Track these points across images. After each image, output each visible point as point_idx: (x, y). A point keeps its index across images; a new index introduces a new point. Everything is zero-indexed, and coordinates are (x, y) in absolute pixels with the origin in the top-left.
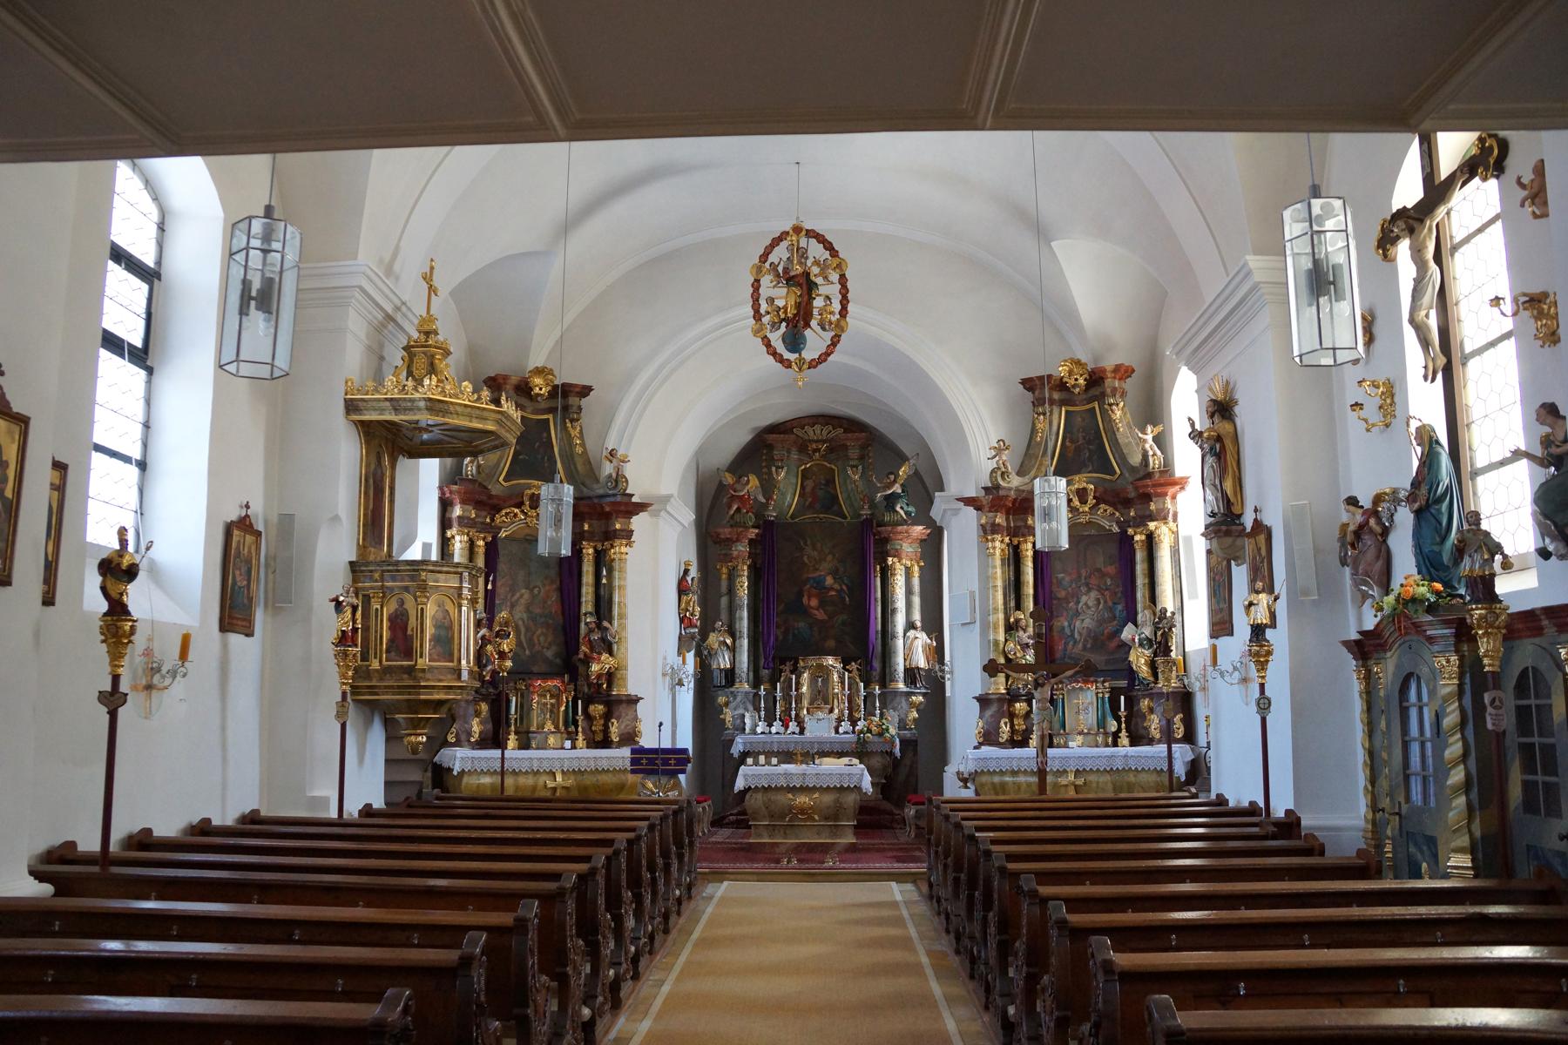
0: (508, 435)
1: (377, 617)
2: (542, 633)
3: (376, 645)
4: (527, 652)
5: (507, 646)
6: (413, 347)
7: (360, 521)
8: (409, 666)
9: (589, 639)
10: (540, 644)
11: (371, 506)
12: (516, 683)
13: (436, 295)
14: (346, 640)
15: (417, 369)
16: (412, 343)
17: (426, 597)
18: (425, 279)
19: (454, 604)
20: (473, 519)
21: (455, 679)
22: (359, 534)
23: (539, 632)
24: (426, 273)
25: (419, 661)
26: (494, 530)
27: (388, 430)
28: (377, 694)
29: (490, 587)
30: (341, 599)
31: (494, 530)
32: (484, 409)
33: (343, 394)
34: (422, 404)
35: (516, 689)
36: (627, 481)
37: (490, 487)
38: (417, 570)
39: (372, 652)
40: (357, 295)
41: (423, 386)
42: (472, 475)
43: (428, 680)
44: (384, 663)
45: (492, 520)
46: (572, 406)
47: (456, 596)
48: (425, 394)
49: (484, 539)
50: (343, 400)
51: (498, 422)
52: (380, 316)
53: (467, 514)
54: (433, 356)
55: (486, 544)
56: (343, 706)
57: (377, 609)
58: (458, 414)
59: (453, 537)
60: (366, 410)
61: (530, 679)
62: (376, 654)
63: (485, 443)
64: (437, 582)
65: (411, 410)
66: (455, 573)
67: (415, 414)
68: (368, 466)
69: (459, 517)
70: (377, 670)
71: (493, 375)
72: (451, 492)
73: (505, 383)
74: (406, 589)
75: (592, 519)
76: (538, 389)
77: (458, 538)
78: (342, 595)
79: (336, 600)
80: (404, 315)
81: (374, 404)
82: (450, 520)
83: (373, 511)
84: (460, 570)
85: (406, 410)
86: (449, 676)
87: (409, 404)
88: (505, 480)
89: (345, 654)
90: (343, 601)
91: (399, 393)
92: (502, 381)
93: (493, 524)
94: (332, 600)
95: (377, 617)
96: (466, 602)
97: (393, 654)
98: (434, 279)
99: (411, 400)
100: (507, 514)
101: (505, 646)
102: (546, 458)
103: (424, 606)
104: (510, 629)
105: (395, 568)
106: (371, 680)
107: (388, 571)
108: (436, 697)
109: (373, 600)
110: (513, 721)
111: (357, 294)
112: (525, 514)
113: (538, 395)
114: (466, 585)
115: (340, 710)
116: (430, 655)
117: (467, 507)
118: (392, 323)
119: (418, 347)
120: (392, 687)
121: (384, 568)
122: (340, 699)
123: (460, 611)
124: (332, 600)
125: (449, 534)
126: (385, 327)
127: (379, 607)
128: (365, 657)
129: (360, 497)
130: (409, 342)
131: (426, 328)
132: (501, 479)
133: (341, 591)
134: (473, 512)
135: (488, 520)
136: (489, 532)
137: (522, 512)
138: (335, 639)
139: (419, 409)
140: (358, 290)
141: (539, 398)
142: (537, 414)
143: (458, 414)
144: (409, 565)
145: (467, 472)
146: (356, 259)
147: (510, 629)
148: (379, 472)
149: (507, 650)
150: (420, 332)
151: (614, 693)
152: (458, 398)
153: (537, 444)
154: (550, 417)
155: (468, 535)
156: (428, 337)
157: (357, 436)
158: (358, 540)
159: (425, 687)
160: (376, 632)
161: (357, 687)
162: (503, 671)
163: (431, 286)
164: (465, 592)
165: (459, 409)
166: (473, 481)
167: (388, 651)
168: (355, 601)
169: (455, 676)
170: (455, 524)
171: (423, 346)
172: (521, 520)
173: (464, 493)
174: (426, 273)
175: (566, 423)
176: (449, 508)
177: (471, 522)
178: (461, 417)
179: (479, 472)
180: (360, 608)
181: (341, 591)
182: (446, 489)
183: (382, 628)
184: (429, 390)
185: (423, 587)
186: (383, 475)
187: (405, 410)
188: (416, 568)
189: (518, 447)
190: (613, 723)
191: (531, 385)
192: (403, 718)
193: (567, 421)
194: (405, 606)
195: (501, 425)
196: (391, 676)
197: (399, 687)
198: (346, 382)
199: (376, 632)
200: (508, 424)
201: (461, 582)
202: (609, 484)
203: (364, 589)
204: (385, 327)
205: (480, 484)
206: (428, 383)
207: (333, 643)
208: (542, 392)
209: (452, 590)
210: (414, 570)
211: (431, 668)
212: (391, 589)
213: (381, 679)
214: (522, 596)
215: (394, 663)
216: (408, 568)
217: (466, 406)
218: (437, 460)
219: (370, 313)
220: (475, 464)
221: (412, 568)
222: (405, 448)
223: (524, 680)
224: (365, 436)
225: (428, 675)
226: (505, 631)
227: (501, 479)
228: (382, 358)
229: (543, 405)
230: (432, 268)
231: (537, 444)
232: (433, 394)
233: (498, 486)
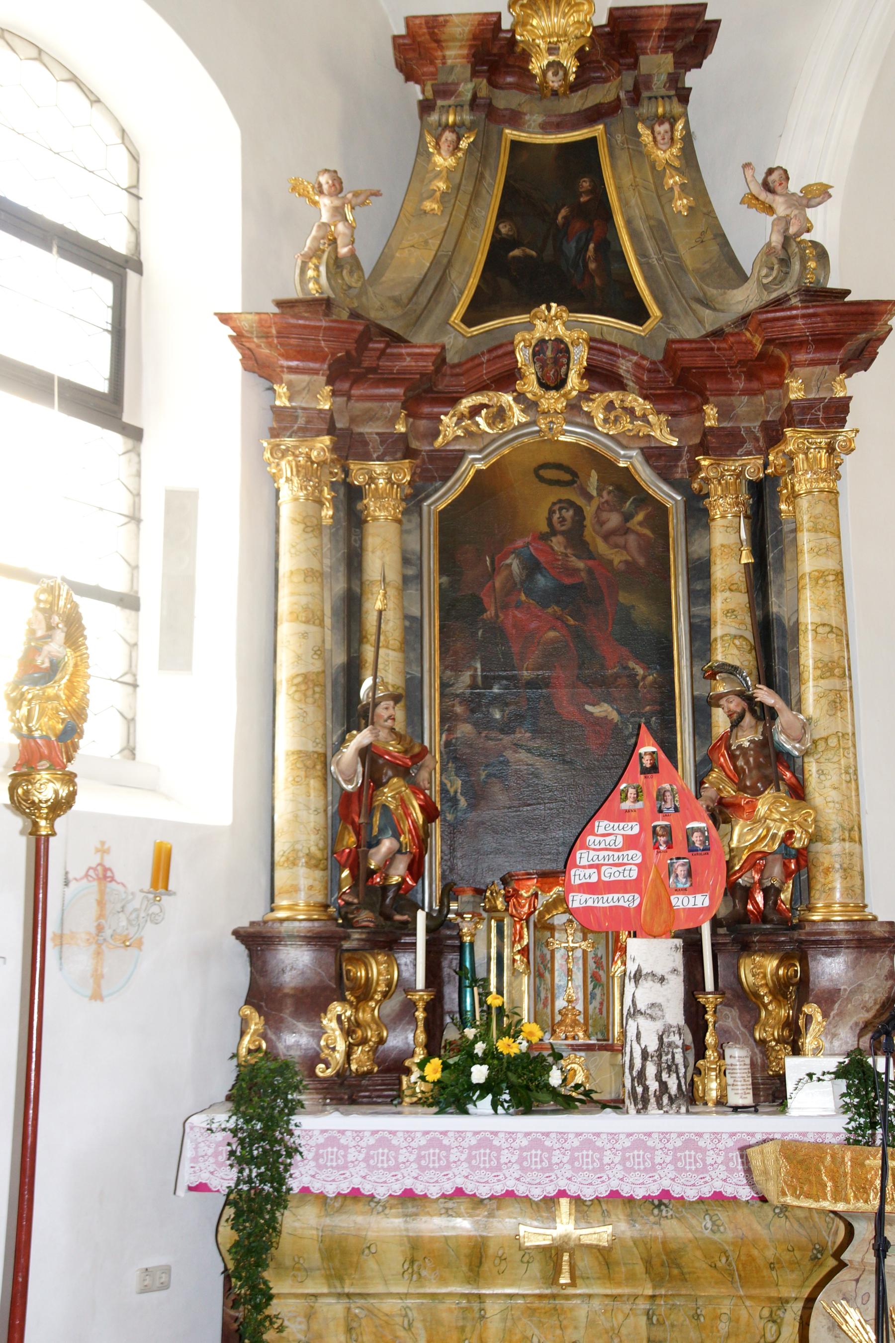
9: (728, 748)
36: (822, 255)
46: (648, 78)
75: (729, 393)
88: (469, 320)
100: (475, 411)
112: (530, 406)
137: (520, 398)
141: (554, 82)
142: (559, 126)
151: (816, 917)
153: (563, 212)
154: (598, 130)
172: (522, 425)
175: (639, 135)
189: (504, 229)
190: (809, 1019)
193: (641, 128)
202: (764, 271)
229: (577, 102)
231: (563, 212)
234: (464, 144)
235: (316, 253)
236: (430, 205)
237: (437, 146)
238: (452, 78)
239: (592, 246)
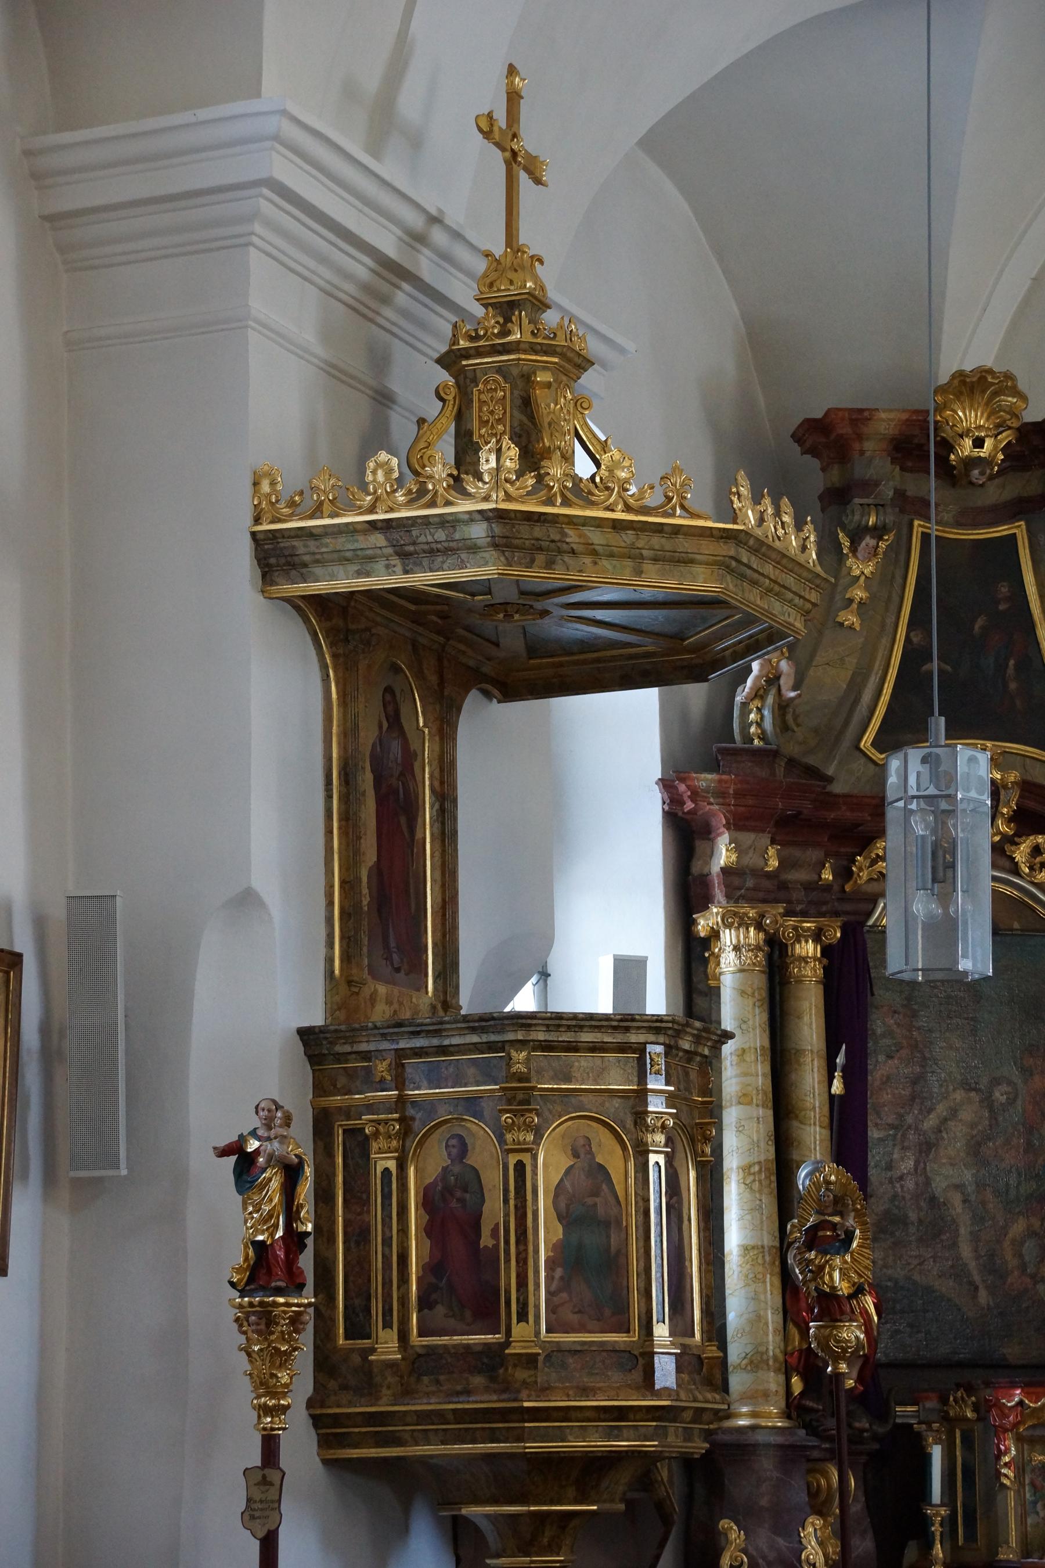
0: (777, 607)
1: (387, 1196)
2: (1031, 1233)
3: (387, 1283)
4: (983, 1296)
5: (844, 1274)
6: (466, 354)
7: (330, 904)
8: (487, 1345)
10: (1023, 1267)
11: (370, 855)
12: (944, 1400)
13: (538, 181)
14: (269, 1273)
15: (484, 423)
16: (463, 343)
17: (528, 1127)
18: (487, 135)
19: (624, 1147)
20: (768, 875)
21: (637, 1388)
22: (330, 945)
23: (1018, 1227)
24: (490, 116)
25: (519, 1330)
26: (848, 907)
27: (417, 619)
28: (394, 1440)
29: (837, 1087)
30: (253, 1145)
31: (848, 907)
32: (677, 530)
33: (249, 520)
34: (478, 531)
35: (946, 1418)
37: (830, 771)
38: (500, 1046)
39: (377, 1308)
40: (265, 207)
41: (479, 476)
42: (763, 737)
43: (544, 1391)
44: (416, 1340)
45: (845, 873)
47: (629, 1123)
48: (486, 499)
49: (817, 936)
50: (248, 540)
51: (729, 567)
52: (361, 268)
53: (752, 860)
54: (527, 378)
55: (827, 951)
56: (265, 1482)
57: (387, 1170)
58: (594, 553)
59: (715, 934)
60: (317, 561)
61: (988, 1384)
62: (387, 1312)
63: (721, 637)
64: (568, 1079)
65: (448, 551)
66: (623, 1048)
67: (462, 566)
68: (350, 732)
69: (725, 871)
70: (391, 1365)
71: (819, 415)
72: (695, 795)
73: (860, 437)
74: (471, 1104)
76: (968, 442)
77: (728, 937)
78: (254, 1134)
79: (235, 1149)
80: (445, 257)
81: (342, 543)
82: (704, 881)
83: (379, 871)
84: (634, 1038)
85: (435, 554)
86: (616, 1377)
87: (441, 535)
89: (266, 1317)
90: (257, 1152)
91: (410, 503)
92: (845, 430)
93: (848, 888)
94: (224, 1152)
95: (387, 1196)
96: (660, 1138)
97: (440, 1310)
98: (523, 132)
99: (444, 522)
101: (836, 1275)
102: (1011, 670)
103: (526, 1158)
104: (851, 1222)
105: (435, 1042)
106: (375, 1399)
107: (418, 1052)
108: (577, 1445)
109: (374, 1146)
110: (936, 1528)
111: (267, 205)
113: (971, 463)
114: (656, 1083)
115: (257, 1495)
116: (551, 1309)
117: (748, 838)
118: (406, 286)
119: (479, 353)
120: (439, 1416)
121: (402, 1044)
122: (256, 1460)
123: (643, 1168)
124: (224, 1152)
125: (703, 924)
126: (385, 300)
127: (392, 1165)
128: (358, 1328)
129: (329, 832)
130: (454, 341)
131: (505, 291)
132: (867, 741)
133: (255, 1122)
134: (771, 851)
135: (827, 875)
136: (836, 914)
138: (239, 1270)
139: (473, 548)
140: (265, 191)
143: (594, 553)
144: (473, 1030)
145: (745, 726)
146: (258, 95)
147: (851, 1222)
148: (396, 748)
149: (844, 1288)
150: (485, 306)
152: (592, 504)
154: (1019, 529)
155: (759, 927)
156: (508, 320)
157: (308, 638)
158: (330, 960)
159: (536, 1414)
160: (387, 1242)
161: (337, 1420)
162: (837, 1358)
163: (514, 154)
164: (656, 1105)
165: (596, 537)
166: (768, 755)
167: (425, 1303)
168: (291, 1151)
169: (637, 1376)
170: (719, 894)
171: (495, 350)
173: (738, 794)
174: (490, 116)
176: (700, 845)
177: (767, 884)
178: (605, 563)
179: (783, 725)
180: (308, 1171)
181: (255, 1122)
182: (682, 788)
183: (404, 1231)
184: (497, 486)
185: (520, 1096)
186: (410, 759)
187: (432, 552)
188: (493, 1038)
191: (947, 433)
192: (487, 1516)
194: (470, 1160)
195: (742, 577)
196: (438, 1382)
197: (460, 1416)
198: (256, 484)
199: (387, 1242)
200: (769, 569)
201: (642, 1078)
203: (347, 1112)
204: (385, 300)
205: (792, 762)
206: (493, 464)
207: (233, 1284)
208: (985, 452)
209: (617, 1103)
210: (491, 1047)
211: (556, 1354)
212: (429, 1106)
213: (407, 1393)
214: (954, 1112)
215: (445, 1340)
216: (475, 1039)
217: (617, 526)
218: (655, 691)
219: (323, 260)
220: (770, 700)
221: (485, 1038)
222: (487, 669)
223: (970, 1389)
224: (332, 645)
225: (544, 1375)
226: (834, 1226)
227: (867, 741)
228: (384, 399)
229: (994, 494)
230: (514, 97)
232: (508, 497)
233: (859, 765)
234: (883, 545)
235: (758, 694)
236: (850, 618)
237: (854, 549)
238: (871, 473)
239: (1012, 662)
